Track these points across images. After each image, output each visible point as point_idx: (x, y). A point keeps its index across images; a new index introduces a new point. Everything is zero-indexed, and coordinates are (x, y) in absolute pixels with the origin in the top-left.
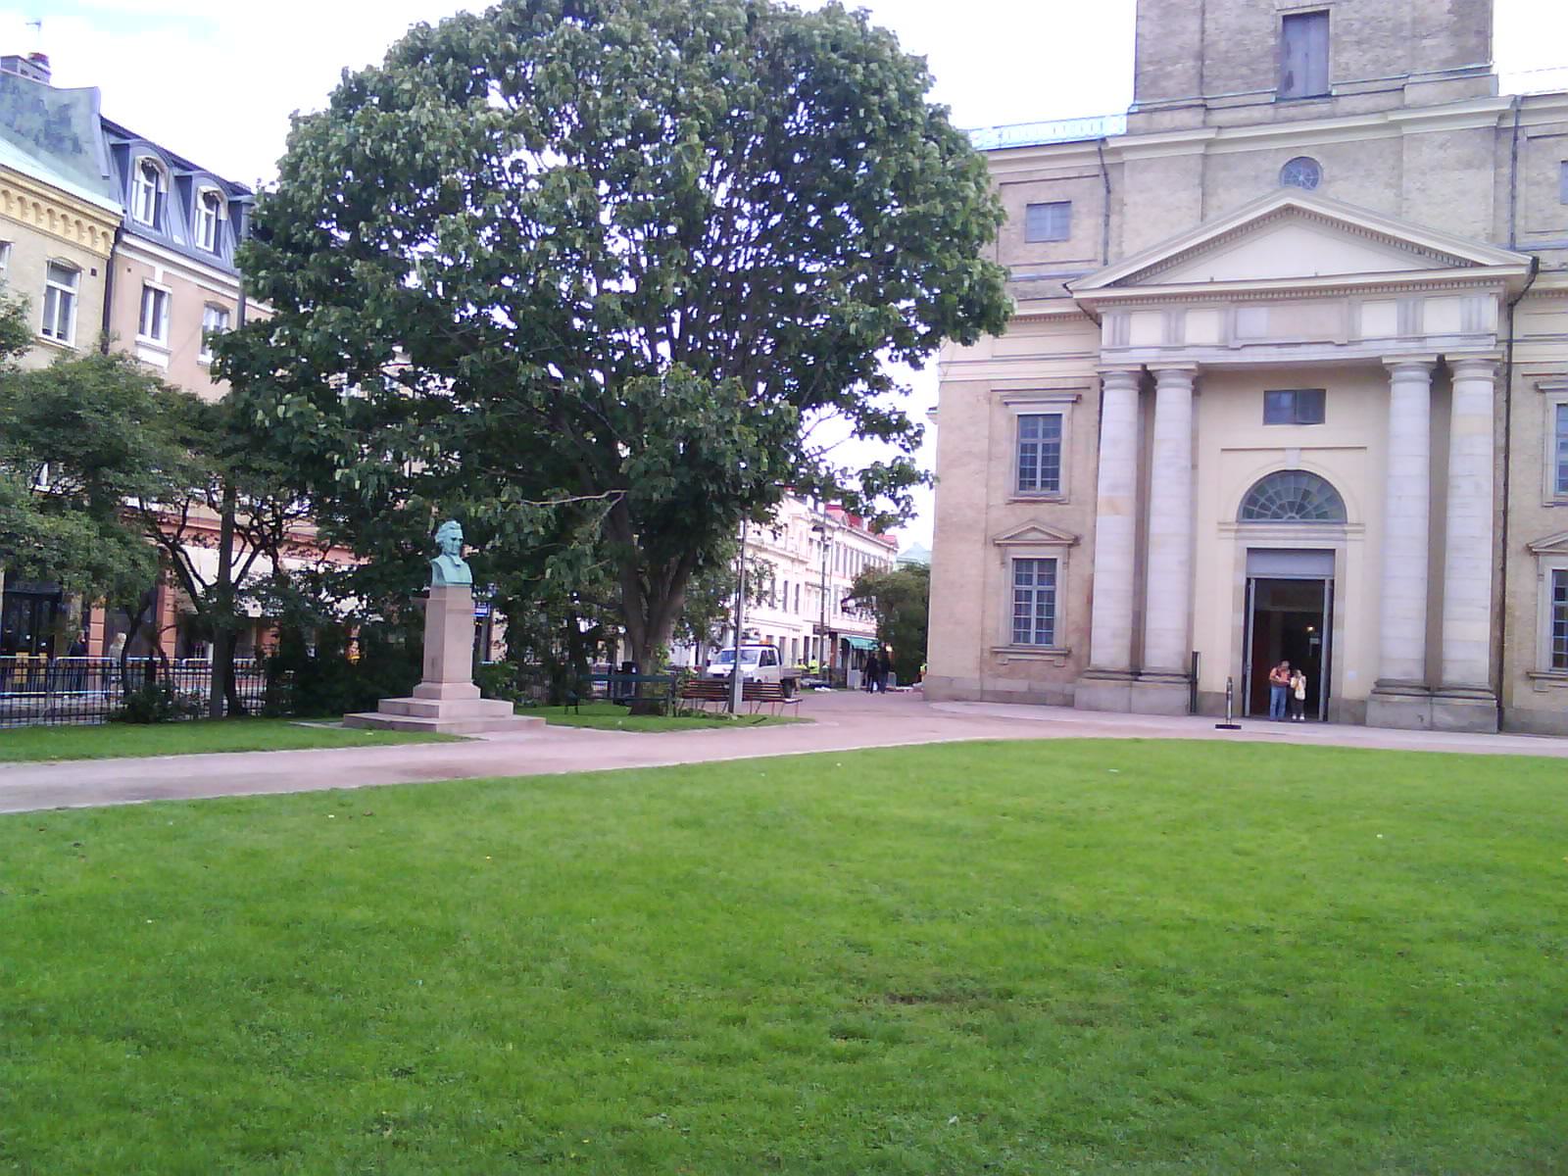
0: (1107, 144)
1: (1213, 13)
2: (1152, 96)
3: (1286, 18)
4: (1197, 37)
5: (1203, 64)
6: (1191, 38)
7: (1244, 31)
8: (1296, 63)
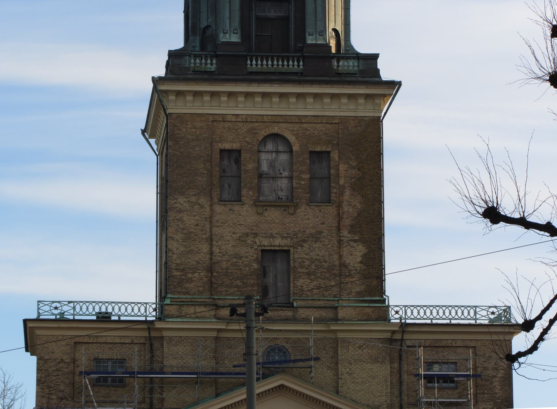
0: (155, 325)
1: (217, 242)
2: (179, 293)
3: (263, 251)
4: (208, 256)
5: (212, 275)
6: (203, 256)
7: (238, 256)
8: (270, 280)
